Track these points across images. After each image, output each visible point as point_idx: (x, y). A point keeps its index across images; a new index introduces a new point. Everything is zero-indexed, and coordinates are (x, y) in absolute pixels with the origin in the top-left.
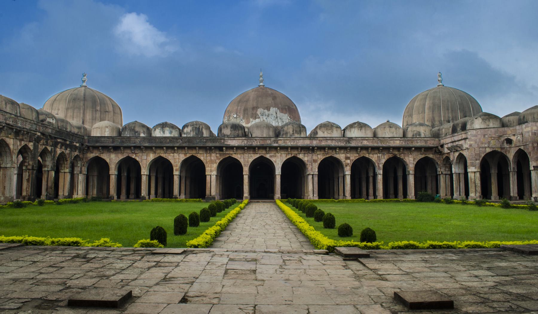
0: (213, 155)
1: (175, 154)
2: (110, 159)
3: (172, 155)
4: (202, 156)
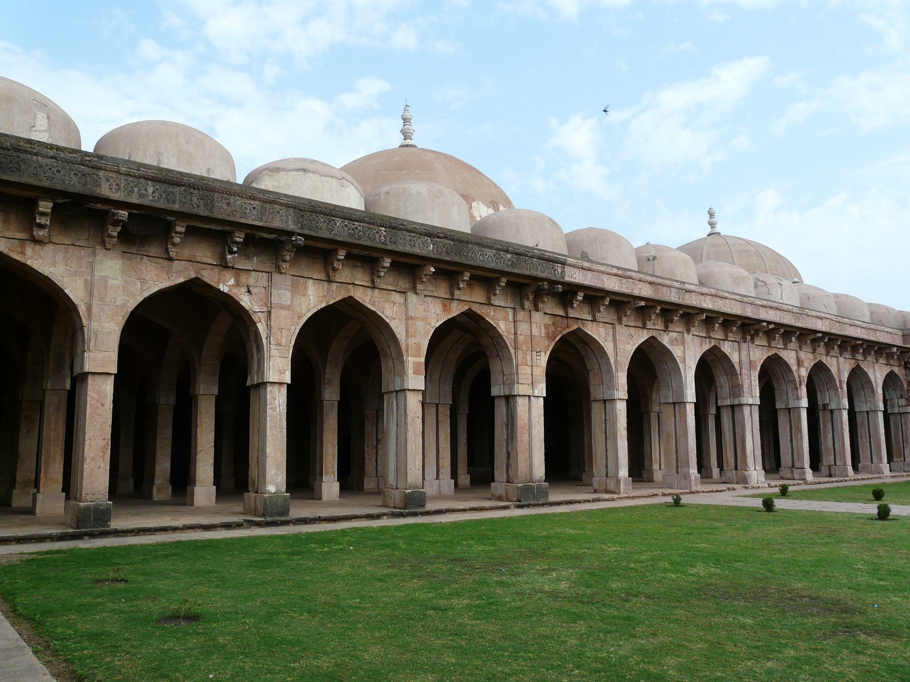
0: (537, 316)
1: (412, 298)
2: (90, 287)
3: (397, 298)
4: (502, 318)
